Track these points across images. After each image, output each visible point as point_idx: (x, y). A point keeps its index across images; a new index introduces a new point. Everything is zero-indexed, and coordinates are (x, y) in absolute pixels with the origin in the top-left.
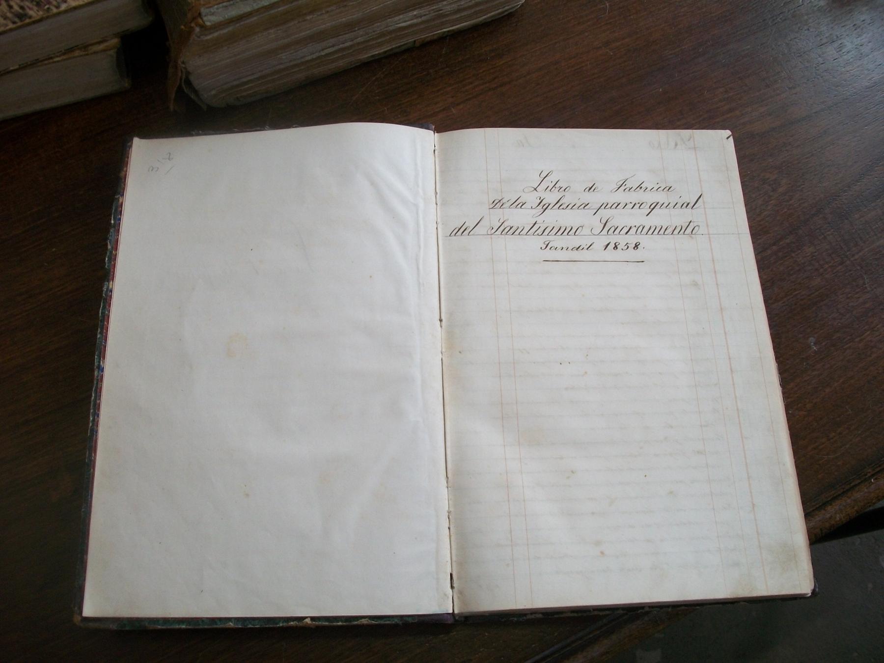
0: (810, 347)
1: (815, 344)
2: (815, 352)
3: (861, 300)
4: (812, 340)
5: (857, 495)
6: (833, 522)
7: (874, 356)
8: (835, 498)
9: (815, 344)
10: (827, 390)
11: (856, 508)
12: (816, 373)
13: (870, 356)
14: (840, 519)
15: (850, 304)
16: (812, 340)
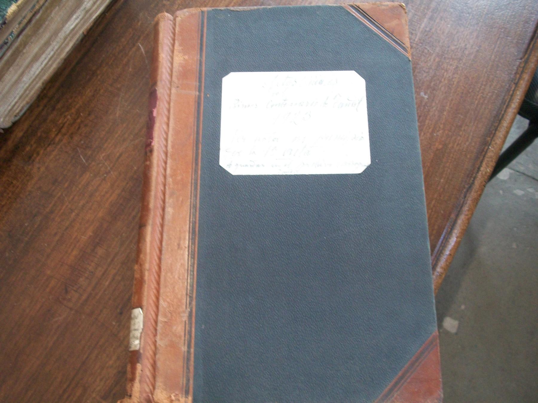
0: (423, 98)
1: (425, 94)
2: (428, 99)
3: (432, 60)
4: (422, 94)
5: (490, 154)
6: (488, 174)
7: (455, 83)
8: (481, 162)
9: (425, 94)
10: (445, 113)
11: (494, 161)
12: (434, 108)
13: (453, 84)
14: (490, 170)
15: (429, 65)
16: (422, 94)
